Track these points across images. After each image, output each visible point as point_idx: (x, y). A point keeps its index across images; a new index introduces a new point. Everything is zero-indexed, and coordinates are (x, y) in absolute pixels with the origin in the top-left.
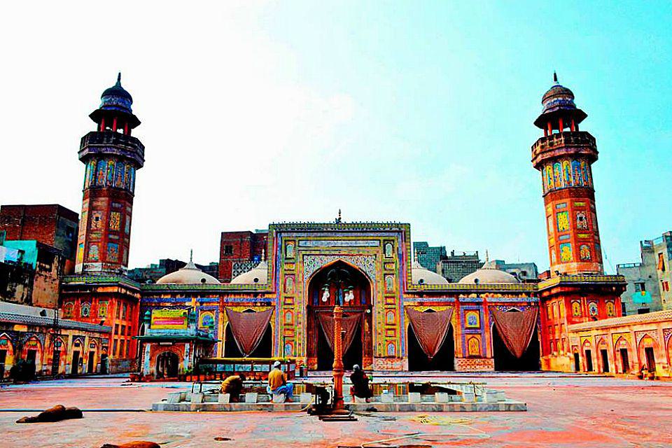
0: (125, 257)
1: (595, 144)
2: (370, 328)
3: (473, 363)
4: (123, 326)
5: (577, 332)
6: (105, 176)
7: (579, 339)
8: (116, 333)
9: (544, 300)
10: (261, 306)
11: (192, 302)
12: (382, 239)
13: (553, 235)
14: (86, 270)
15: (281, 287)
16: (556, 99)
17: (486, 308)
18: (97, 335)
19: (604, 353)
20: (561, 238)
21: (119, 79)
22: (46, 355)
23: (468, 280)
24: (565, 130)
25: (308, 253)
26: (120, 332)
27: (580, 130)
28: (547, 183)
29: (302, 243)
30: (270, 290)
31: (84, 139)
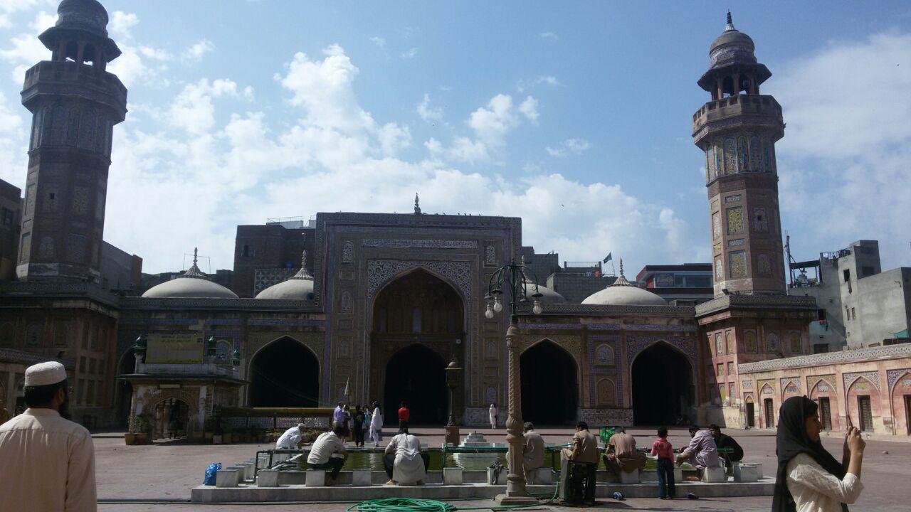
4: (93, 360)
5: (752, 373)
7: (755, 384)
8: (82, 370)
11: (200, 325)
13: (721, 239)
14: (35, 274)
16: (729, 49)
20: (732, 243)
26: (87, 368)
28: (714, 166)
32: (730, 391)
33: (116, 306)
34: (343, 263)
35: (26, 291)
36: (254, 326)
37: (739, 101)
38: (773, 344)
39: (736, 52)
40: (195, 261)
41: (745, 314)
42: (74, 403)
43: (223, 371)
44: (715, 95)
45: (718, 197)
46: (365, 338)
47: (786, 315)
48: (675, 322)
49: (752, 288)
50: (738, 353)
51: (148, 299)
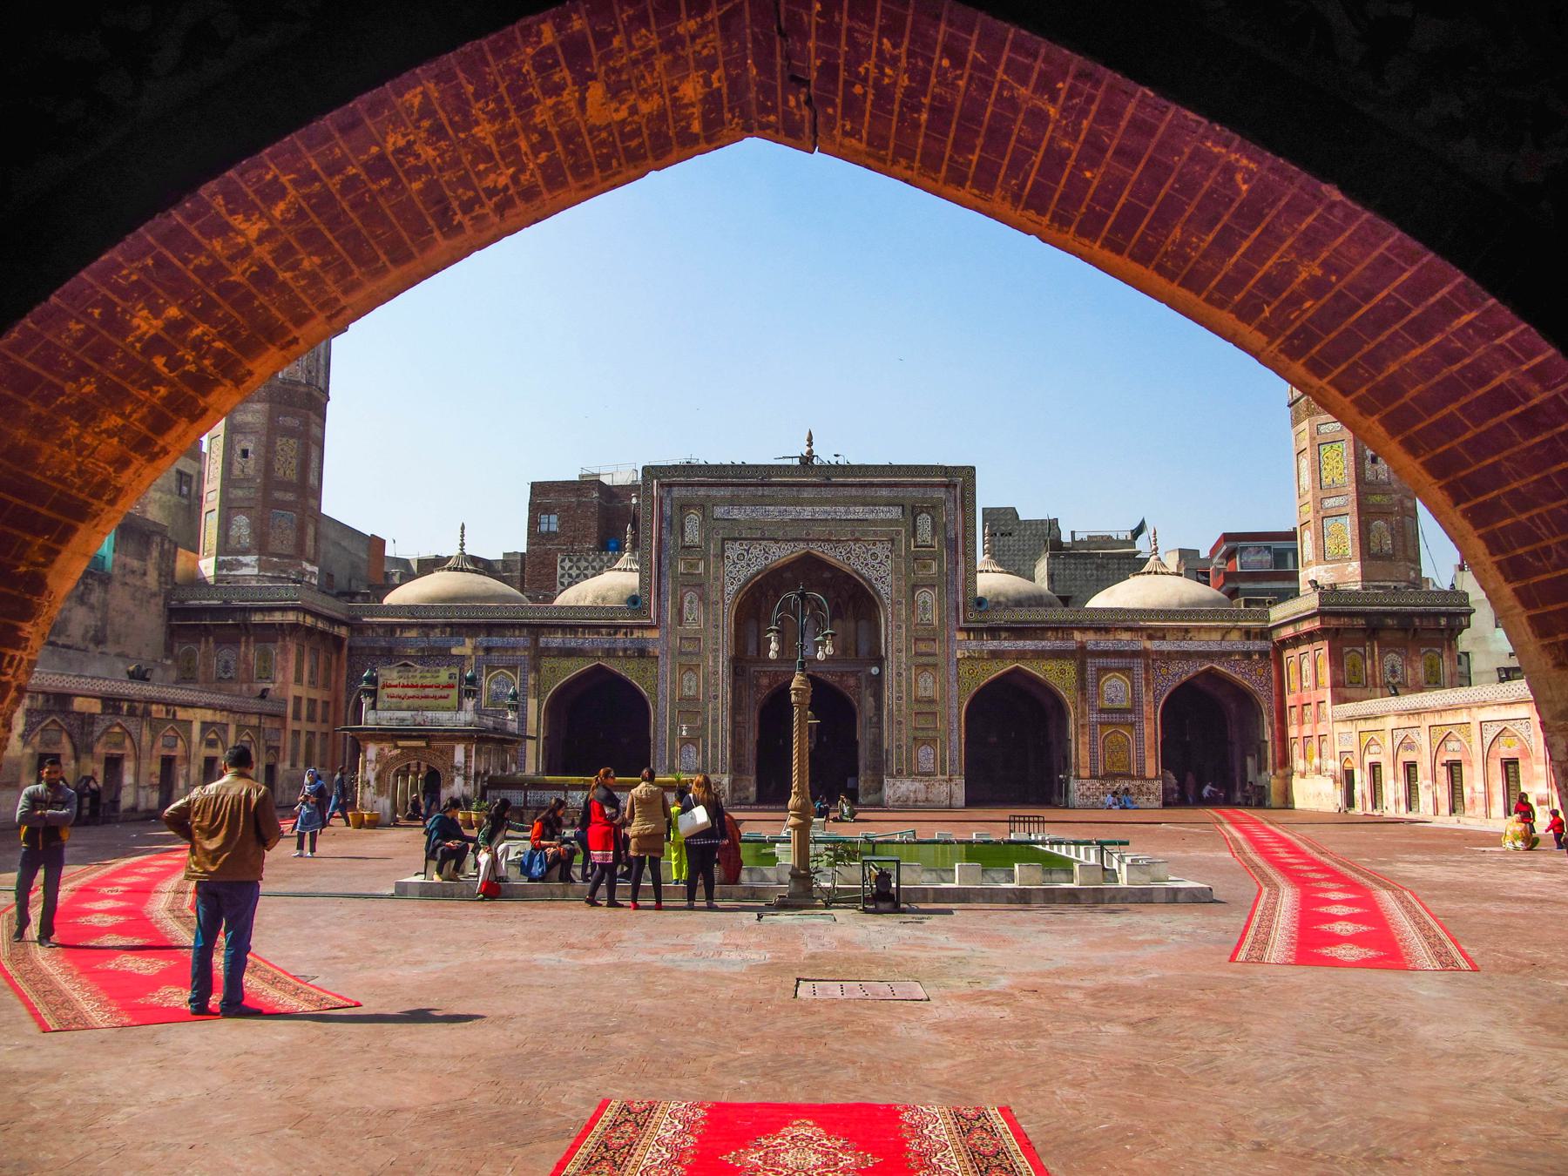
2: (879, 707)
4: (312, 702)
5: (1351, 719)
7: (1355, 736)
8: (297, 717)
9: (1283, 644)
10: (626, 656)
11: (465, 648)
13: (1309, 497)
15: (669, 617)
18: (254, 721)
19: (1410, 767)
20: (1329, 503)
22: (144, 763)
29: (719, 512)
32: (1320, 750)
33: (343, 617)
34: (683, 547)
35: (213, 599)
36: (548, 649)
38: (1394, 672)
40: (462, 545)
41: (1345, 621)
42: (287, 765)
43: (489, 722)
46: (719, 663)
47: (1417, 622)
48: (1235, 636)
49: (1359, 578)
50: (1333, 687)
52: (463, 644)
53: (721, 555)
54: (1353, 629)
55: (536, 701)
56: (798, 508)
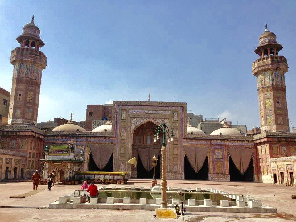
0: (35, 116)
1: (286, 63)
3: (218, 176)
4: (34, 154)
6: (25, 72)
8: (30, 157)
11: (72, 141)
12: (172, 110)
13: (263, 111)
14: (14, 123)
16: (267, 38)
17: (225, 148)
20: (267, 112)
21: (33, 20)
23: (216, 133)
24: (271, 55)
25: (133, 116)
26: (32, 156)
27: (279, 55)
30: (113, 136)
31: (13, 52)
33: (42, 134)
34: (122, 119)
37: (270, 58)
39: (269, 40)
40: (71, 118)
44: (261, 55)
45: (262, 95)
46: (130, 146)
47: (289, 140)
49: (275, 129)
51: (54, 132)
52: (71, 140)
53: (130, 121)
54: (274, 141)
55: (87, 154)
56: (147, 111)
